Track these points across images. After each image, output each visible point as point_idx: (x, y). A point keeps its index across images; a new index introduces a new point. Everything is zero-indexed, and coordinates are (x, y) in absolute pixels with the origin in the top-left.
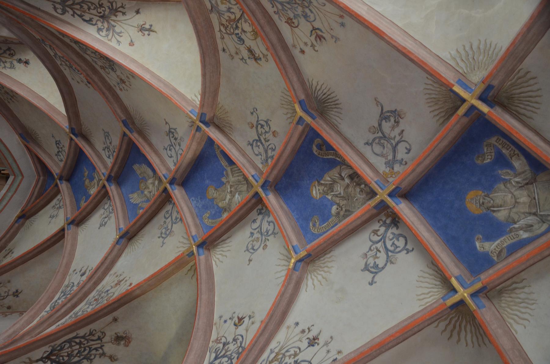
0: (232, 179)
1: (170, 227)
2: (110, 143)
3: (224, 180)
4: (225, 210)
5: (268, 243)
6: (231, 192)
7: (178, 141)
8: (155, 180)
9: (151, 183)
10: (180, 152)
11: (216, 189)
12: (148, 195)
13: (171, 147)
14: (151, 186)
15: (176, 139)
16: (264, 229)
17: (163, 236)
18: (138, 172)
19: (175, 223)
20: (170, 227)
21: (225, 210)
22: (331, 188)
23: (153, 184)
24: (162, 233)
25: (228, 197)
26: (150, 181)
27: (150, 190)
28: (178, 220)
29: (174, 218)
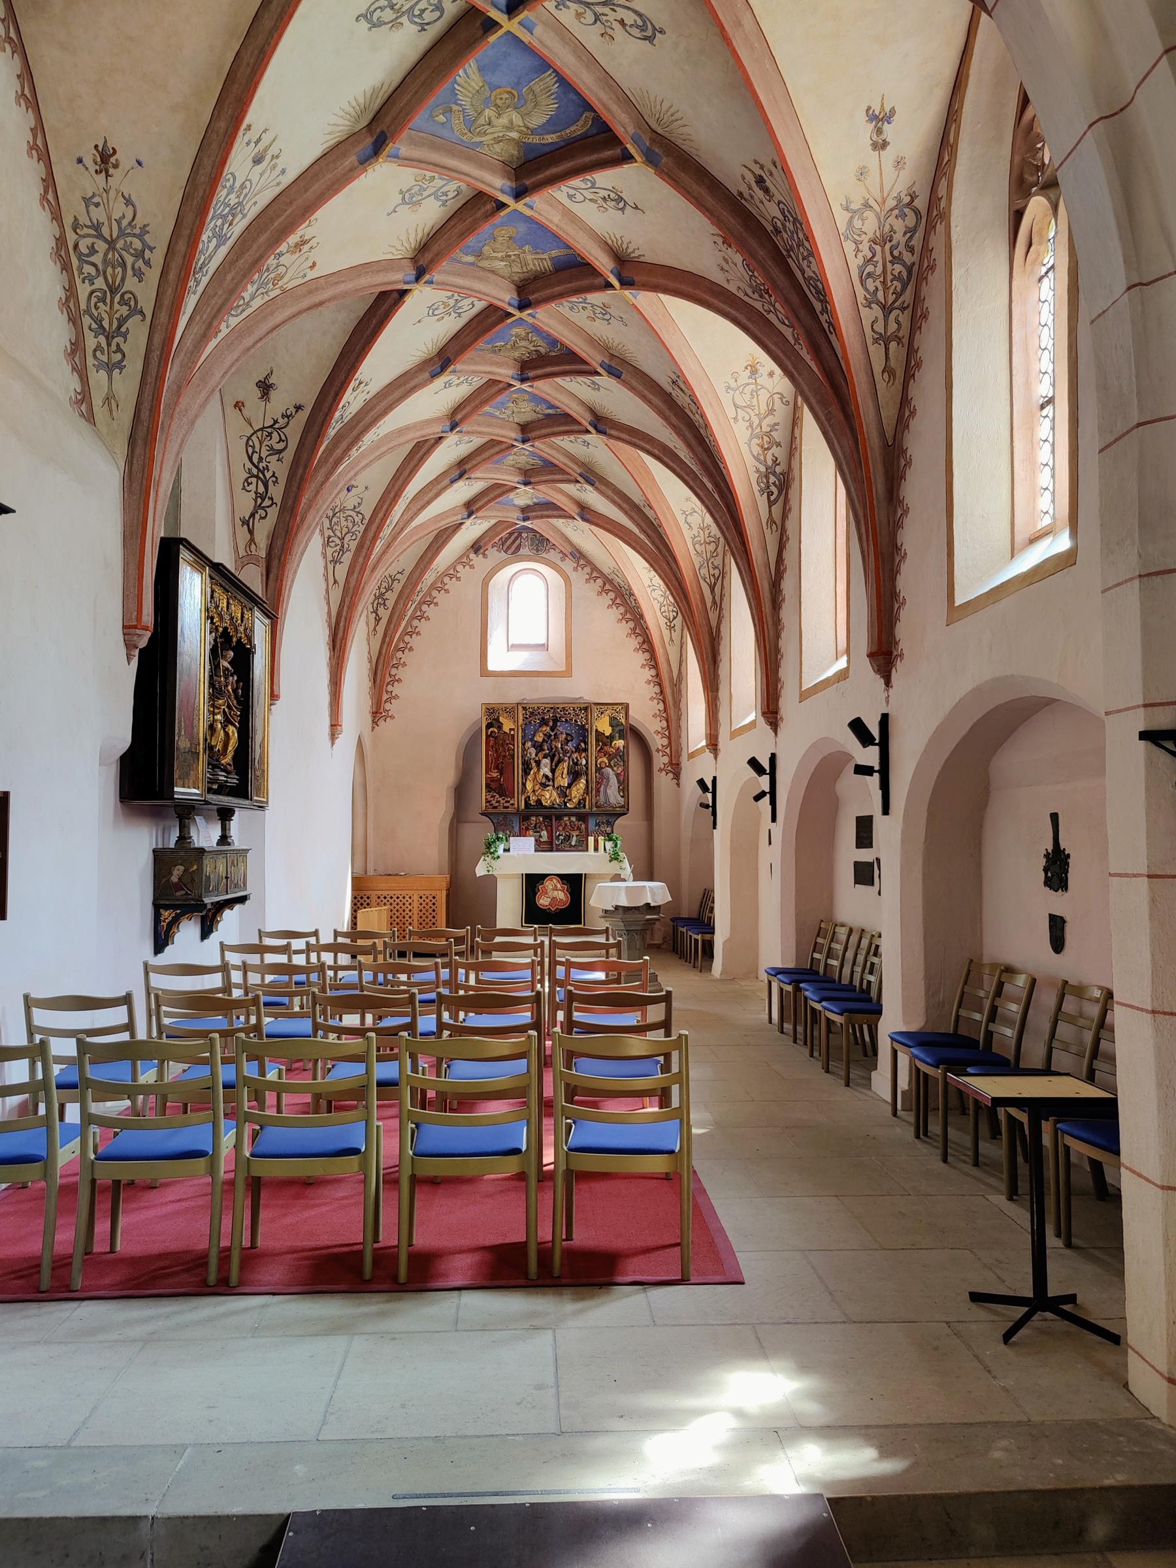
0: (529, 258)
1: (425, 194)
2: (622, 22)
3: (527, 248)
4: (479, 255)
5: (446, 318)
6: (509, 256)
7: (600, 201)
8: (520, 132)
9: (511, 122)
10: (579, 197)
11: (510, 238)
12: (481, 121)
13: (590, 185)
14: (504, 121)
15: (604, 199)
16: (460, 305)
17: (407, 195)
18: (537, 85)
19: (437, 198)
20: (425, 194)
21: (479, 255)
22: (526, 339)
23: (510, 127)
24: (408, 191)
25: (499, 255)
26: (516, 119)
27: (495, 121)
28: (444, 198)
29: (444, 189)
